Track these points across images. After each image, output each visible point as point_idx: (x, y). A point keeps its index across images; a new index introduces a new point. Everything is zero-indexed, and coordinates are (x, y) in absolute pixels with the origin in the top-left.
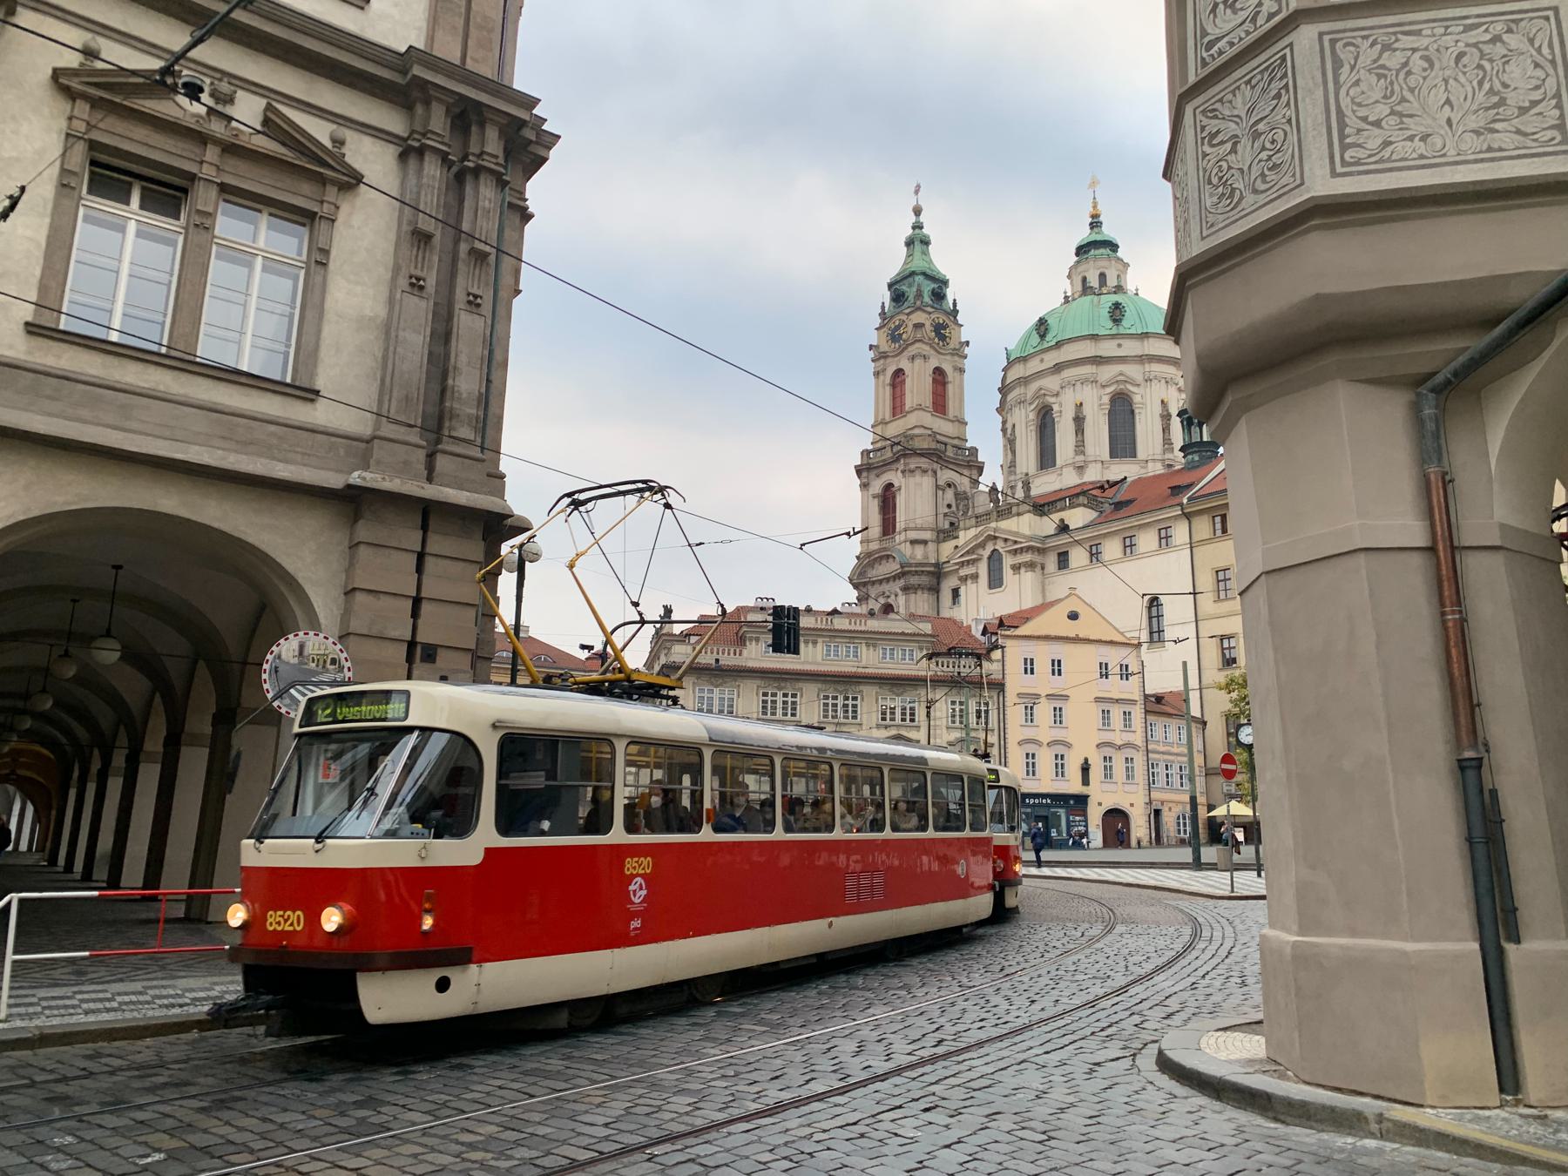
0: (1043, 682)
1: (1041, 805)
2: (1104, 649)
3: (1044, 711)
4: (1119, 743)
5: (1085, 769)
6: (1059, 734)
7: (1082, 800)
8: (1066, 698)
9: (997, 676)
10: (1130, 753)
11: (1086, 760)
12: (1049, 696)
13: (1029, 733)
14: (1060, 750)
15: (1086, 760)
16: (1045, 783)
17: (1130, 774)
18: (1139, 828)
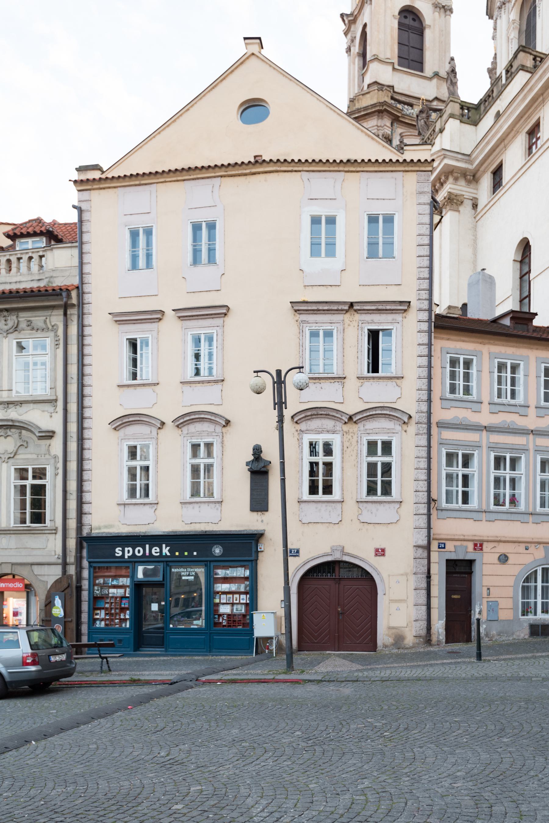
0: (173, 282)
1: (146, 560)
2: (323, 184)
3: (169, 348)
4: (351, 408)
5: (259, 471)
6: (202, 399)
7: (243, 547)
8: (221, 312)
9: (67, 279)
10: (379, 430)
11: (257, 451)
12: (186, 314)
13: (136, 401)
14: (202, 433)
15: (257, 451)
16: (171, 513)
17: (379, 481)
18: (402, 608)
